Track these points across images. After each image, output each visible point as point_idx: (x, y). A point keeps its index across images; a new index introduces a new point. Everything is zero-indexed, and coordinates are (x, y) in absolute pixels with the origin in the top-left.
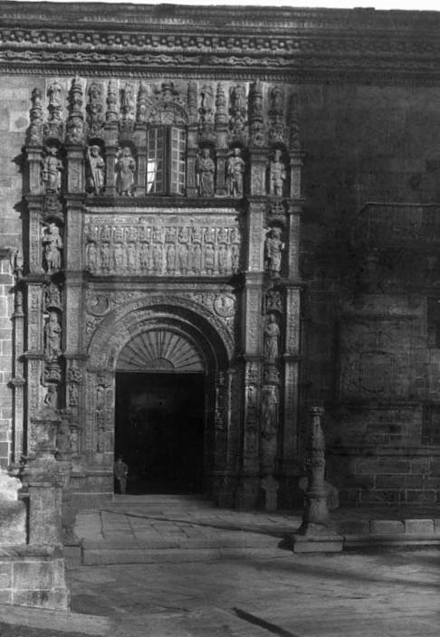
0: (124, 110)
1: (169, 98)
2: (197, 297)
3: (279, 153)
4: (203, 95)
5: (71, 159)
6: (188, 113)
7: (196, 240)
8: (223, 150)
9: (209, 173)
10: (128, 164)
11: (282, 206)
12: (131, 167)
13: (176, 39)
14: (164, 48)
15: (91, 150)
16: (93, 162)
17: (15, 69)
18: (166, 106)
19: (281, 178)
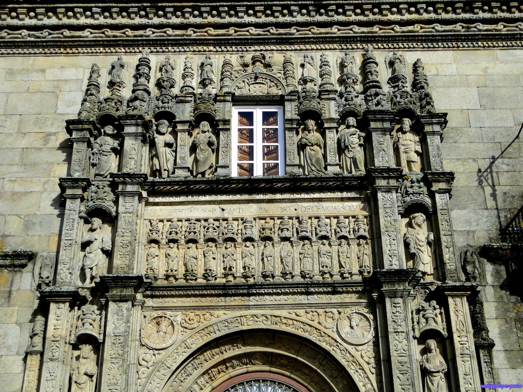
0: (203, 83)
1: (259, 68)
2: (309, 316)
3: (407, 123)
4: (303, 66)
5: (129, 134)
6: (285, 84)
7: (304, 234)
8: (331, 120)
9: (315, 148)
10: (206, 140)
11: (422, 184)
12: (210, 144)
13: (266, 9)
14: (253, 19)
15: (157, 126)
16: (160, 140)
17: (71, 47)
18: (256, 78)
19: (416, 152)
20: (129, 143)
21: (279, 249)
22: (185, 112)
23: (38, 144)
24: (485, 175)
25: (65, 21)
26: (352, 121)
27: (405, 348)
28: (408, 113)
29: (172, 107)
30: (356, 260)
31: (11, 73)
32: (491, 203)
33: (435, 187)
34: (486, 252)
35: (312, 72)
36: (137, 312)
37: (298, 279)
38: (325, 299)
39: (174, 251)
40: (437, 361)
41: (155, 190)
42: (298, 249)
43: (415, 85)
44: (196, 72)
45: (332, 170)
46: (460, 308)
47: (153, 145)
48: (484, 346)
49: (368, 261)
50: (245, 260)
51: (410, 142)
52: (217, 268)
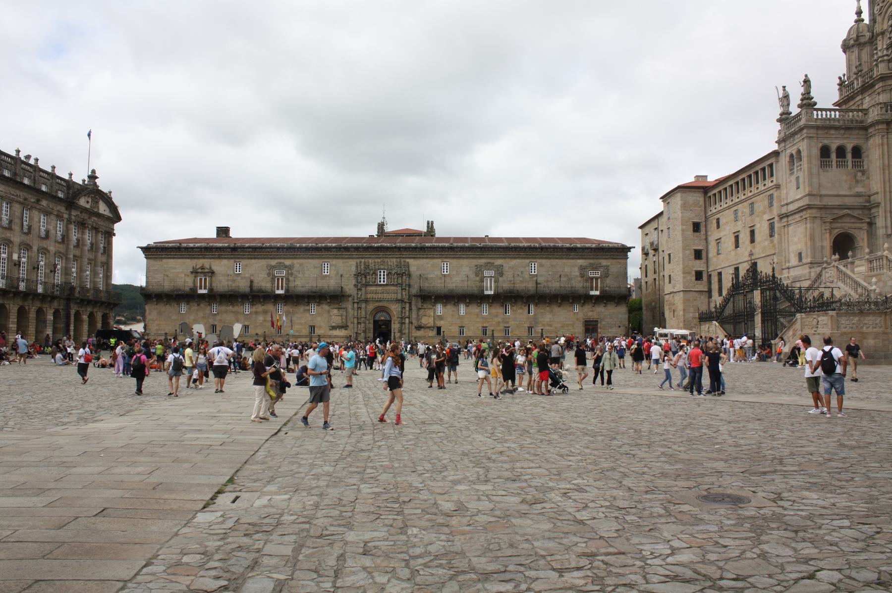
48: (410, 309)
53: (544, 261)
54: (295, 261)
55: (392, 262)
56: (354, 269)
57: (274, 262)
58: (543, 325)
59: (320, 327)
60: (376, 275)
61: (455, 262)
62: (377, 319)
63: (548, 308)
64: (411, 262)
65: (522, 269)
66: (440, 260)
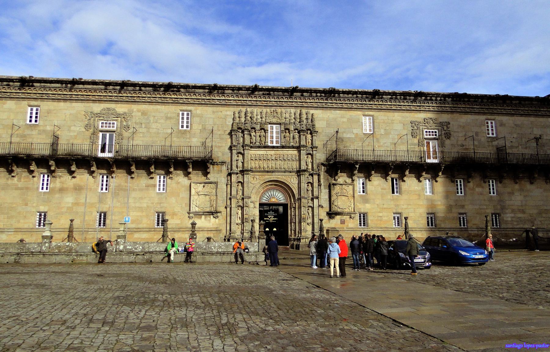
3: (309, 132)
20: (245, 136)
21: (278, 162)
22: (258, 127)
23: (223, 133)
24: (325, 145)
25: (227, 98)
26: (296, 131)
27: (304, 185)
28: (310, 130)
29: (254, 126)
30: (295, 165)
31: (214, 112)
32: (325, 152)
33: (314, 149)
34: (322, 164)
35: (287, 115)
36: (250, 176)
37: (283, 170)
38: (288, 174)
39: (256, 162)
40: (310, 188)
41: (251, 147)
42: (283, 162)
43: (312, 121)
44: (259, 114)
45: (292, 144)
46: (316, 177)
47: (251, 135)
48: (320, 185)
49: (298, 166)
50: (272, 165)
51: (309, 136)
52: (266, 166)
53: (505, 119)
54: (135, 107)
55: (289, 113)
56: (230, 122)
57: (97, 108)
58: (513, 211)
59: (174, 214)
60: (265, 131)
61: (381, 116)
62: (264, 201)
63: (517, 186)
64: (318, 114)
65: (475, 129)
66: (359, 113)
